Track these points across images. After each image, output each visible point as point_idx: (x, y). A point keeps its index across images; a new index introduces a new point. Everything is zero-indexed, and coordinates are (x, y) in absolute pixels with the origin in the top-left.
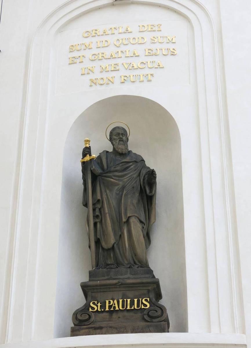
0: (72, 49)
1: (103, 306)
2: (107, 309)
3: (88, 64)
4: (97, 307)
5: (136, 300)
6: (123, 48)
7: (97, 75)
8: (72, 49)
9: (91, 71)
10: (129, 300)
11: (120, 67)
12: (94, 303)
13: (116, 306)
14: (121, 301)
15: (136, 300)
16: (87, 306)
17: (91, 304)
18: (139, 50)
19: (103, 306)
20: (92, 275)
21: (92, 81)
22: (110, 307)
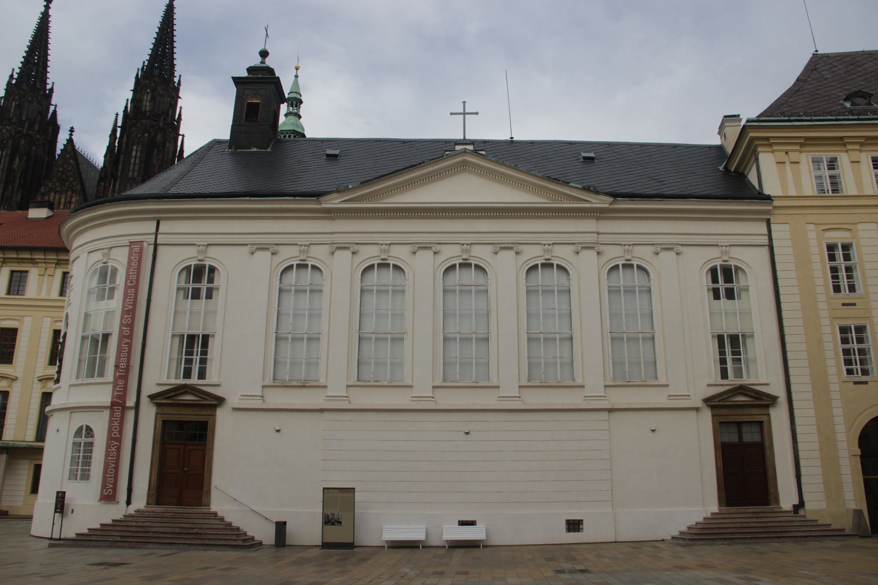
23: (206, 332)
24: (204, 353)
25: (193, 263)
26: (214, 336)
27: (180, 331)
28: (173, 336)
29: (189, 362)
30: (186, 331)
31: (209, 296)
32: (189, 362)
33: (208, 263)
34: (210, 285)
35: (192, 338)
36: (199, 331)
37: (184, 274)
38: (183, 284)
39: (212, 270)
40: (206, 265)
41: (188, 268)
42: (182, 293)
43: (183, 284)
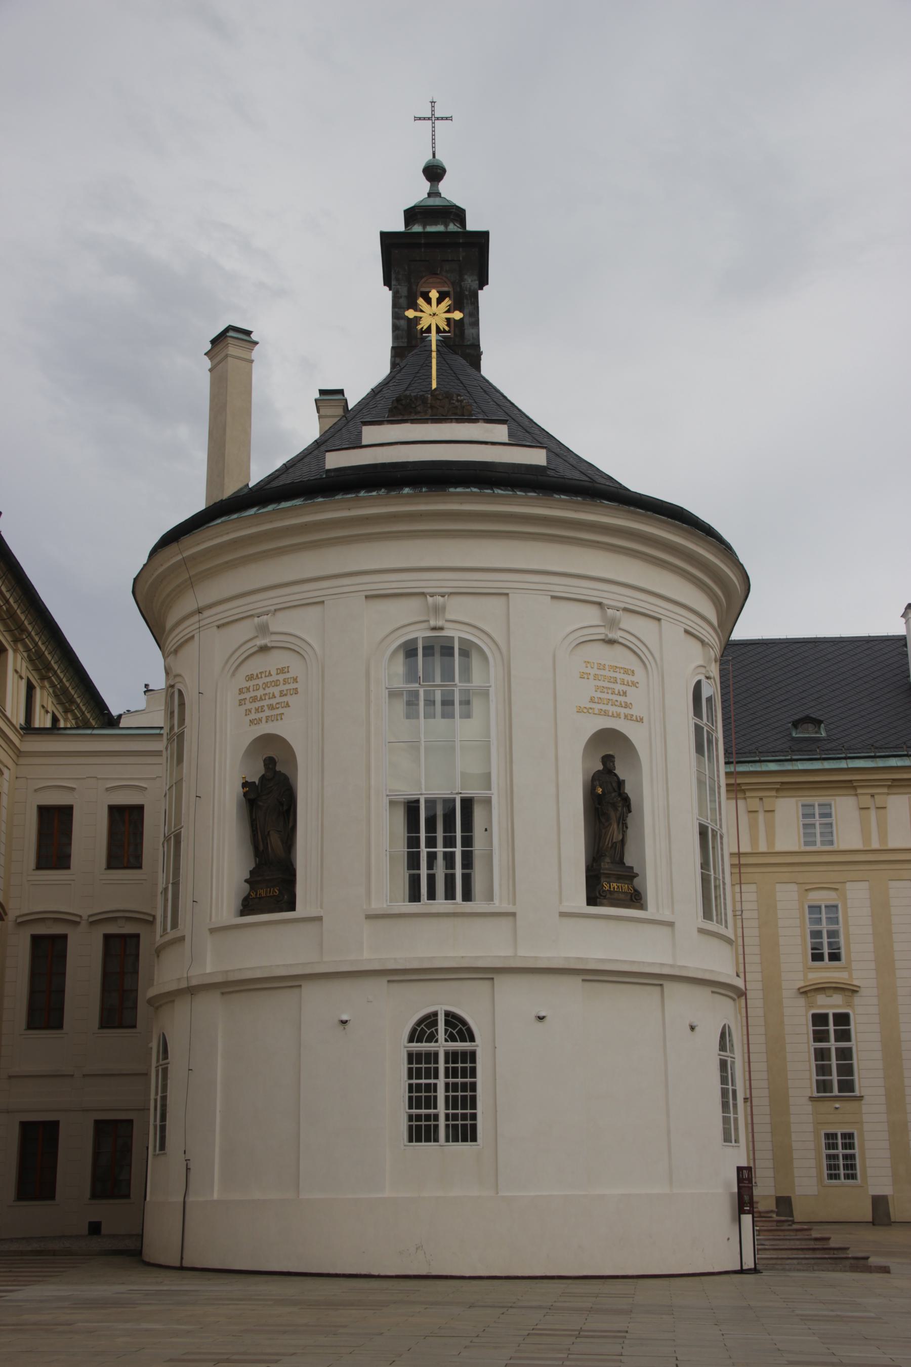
0: (241, 691)
1: (256, 894)
2: (258, 896)
3: (249, 706)
4: (253, 895)
5: (272, 889)
6: (268, 691)
7: (253, 716)
8: (241, 691)
9: (248, 712)
10: (269, 889)
11: (266, 708)
12: (253, 892)
13: (262, 894)
14: (265, 890)
15: (272, 889)
16: (249, 894)
17: (252, 894)
18: (276, 690)
19: (256, 894)
20: (251, 872)
21: (250, 721)
22: (260, 894)
23: (469, 793)
24: (468, 841)
25: (420, 634)
26: (488, 801)
33: (454, 632)
37: (401, 657)
38: (399, 683)
40: (453, 638)
41: (409, 650)
42: (400, 706)
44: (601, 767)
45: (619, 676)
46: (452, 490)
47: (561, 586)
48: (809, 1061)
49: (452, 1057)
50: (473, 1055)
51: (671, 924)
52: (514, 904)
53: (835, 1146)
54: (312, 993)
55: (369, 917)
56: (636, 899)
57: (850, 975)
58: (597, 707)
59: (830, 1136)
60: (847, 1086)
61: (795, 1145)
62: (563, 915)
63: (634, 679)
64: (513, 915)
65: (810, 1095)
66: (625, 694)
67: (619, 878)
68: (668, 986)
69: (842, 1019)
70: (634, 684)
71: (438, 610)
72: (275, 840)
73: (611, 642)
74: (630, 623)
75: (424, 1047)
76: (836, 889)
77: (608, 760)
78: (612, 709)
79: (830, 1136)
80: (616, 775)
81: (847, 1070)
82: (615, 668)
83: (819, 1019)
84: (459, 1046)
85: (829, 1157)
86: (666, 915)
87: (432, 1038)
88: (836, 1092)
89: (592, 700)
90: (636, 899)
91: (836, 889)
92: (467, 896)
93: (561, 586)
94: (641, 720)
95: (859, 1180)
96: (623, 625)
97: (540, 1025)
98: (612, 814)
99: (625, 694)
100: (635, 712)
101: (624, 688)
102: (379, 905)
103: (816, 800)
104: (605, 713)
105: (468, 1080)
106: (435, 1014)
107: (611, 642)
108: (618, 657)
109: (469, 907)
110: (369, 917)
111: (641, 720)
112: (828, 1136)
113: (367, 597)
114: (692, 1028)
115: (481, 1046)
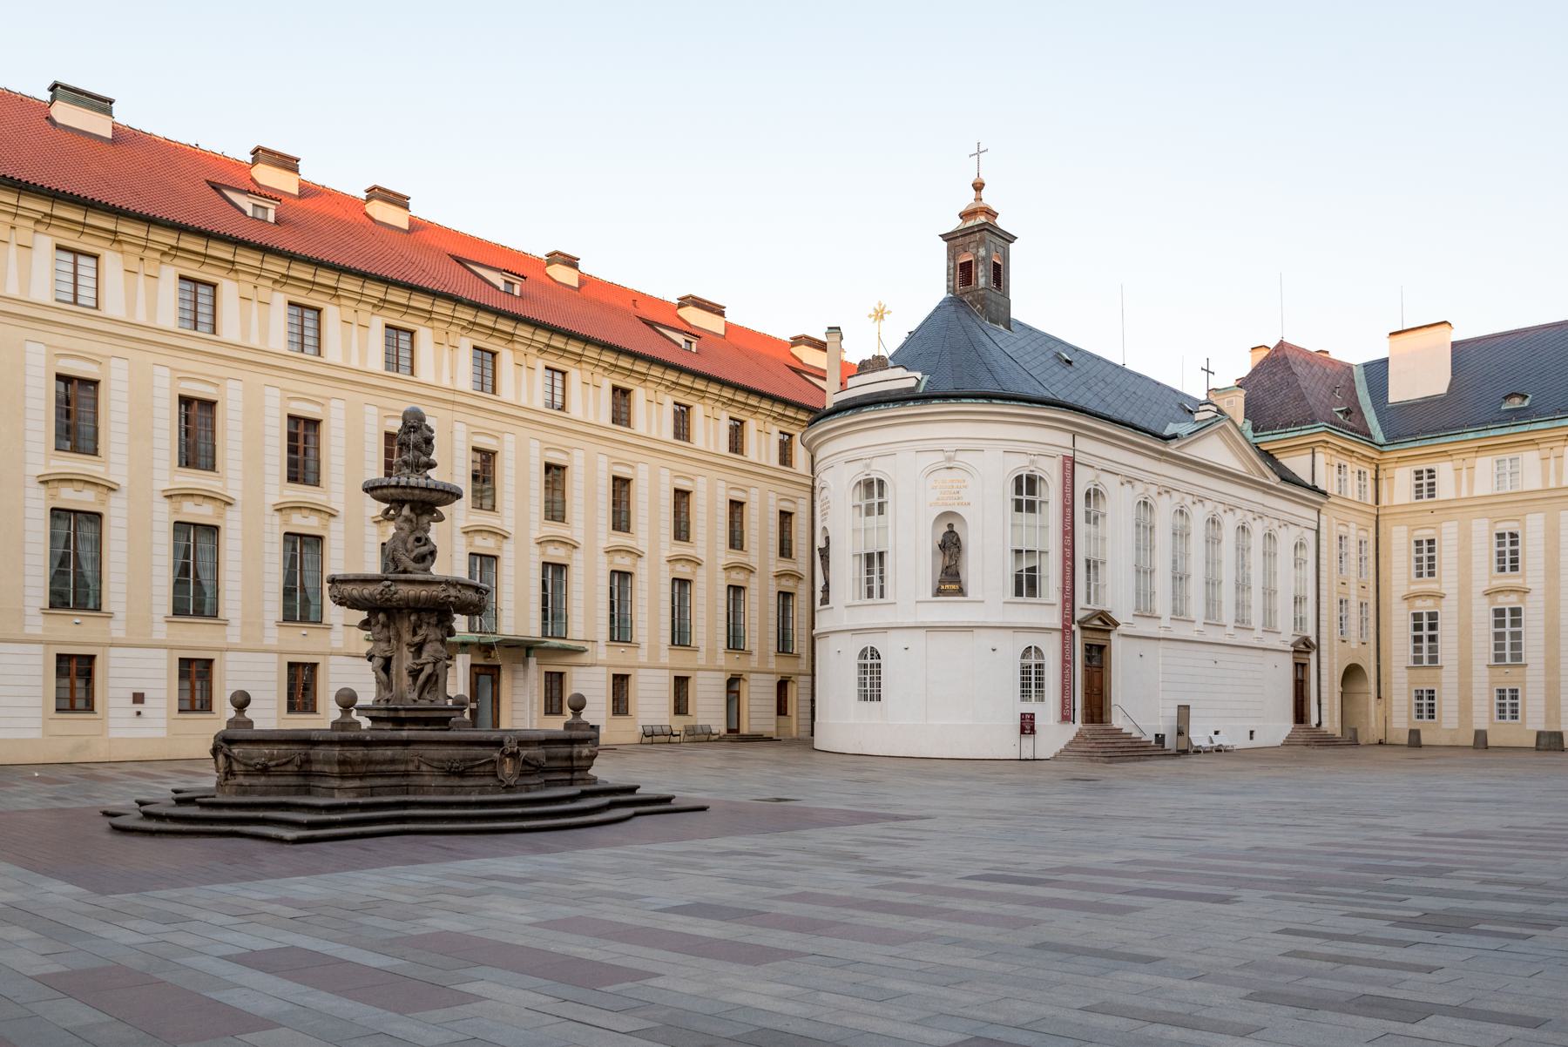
23: (881, 550)
24: (882, 571)
25: (862, 477)
26: (887, 552)
27: (857, 551)
28: (854, 556)
29: (869, 581)
30: (863, 552)
31: (881, 512)
32: (869, 581)
33: (874, 476)
34: (881, 500)
35: (869, 557)
36: (874, 549)
39: (881, 483)
40: (873, 479)
43: (857, 502)
44: (947, 529)
45: (955, 485)
46: (864, 410)
47: (920, 446)
48: (1489, 641)
49: (872, 666)
50: (880, 664)
51: (983, 602)
52: (895, 598)
53: (1504, 698)
54: (832, 637)
55: (847, 607)
56: (961, 592)
57: (1525, 580)
58: (941, 502)
59: (1502, 691)
60: (1517, 657)
61: (1474, 697)
62: (917, 602)
63: (965, 484)
64: (895, 603)
65: (1487, 663)
66: (958, 492)
67: (950, 583)
68: (975, 630)
69: (1516, 612)
70: (965, 487)
71: (868, 466)
72: (826, 572)
73: (951, 468)
74: (960, 456)
75: (863, 661)
76: (1518, 520)
77: (951, 526)
78: (949, 502)
79: (1502, 691)
80: (954, 532)
81: (1516, 646)
82: (952, 481)
83: (1499, 613)
84: (875, 661)
85: (1500, 705)
86: (980, 598)
87: (865, 658)
88: (1508, 660)
89: (938, 499)
90: (961, 592)
91: (1518, 520)
92: (882, 596)
93: (920, 446)
94: (969, 504)
95: (1519, 720)
96: (957, 459)
97: (905, 651)
98: (947, 553)
99: (958, 492)
100: (965, 500)
101: (956, 490)
102: (849, 601)
103: (1506, 455)
104: (946, 505)
105: (1033, 669)
106: (867, 648)
107: (951, 468)
108: (954, 474)
109: (882, 601)
110: (847, 607)
111: (969, 504)
112: (1500, 691)
113: (846, 462)
114: (994, 650)
115: (882, 661)
